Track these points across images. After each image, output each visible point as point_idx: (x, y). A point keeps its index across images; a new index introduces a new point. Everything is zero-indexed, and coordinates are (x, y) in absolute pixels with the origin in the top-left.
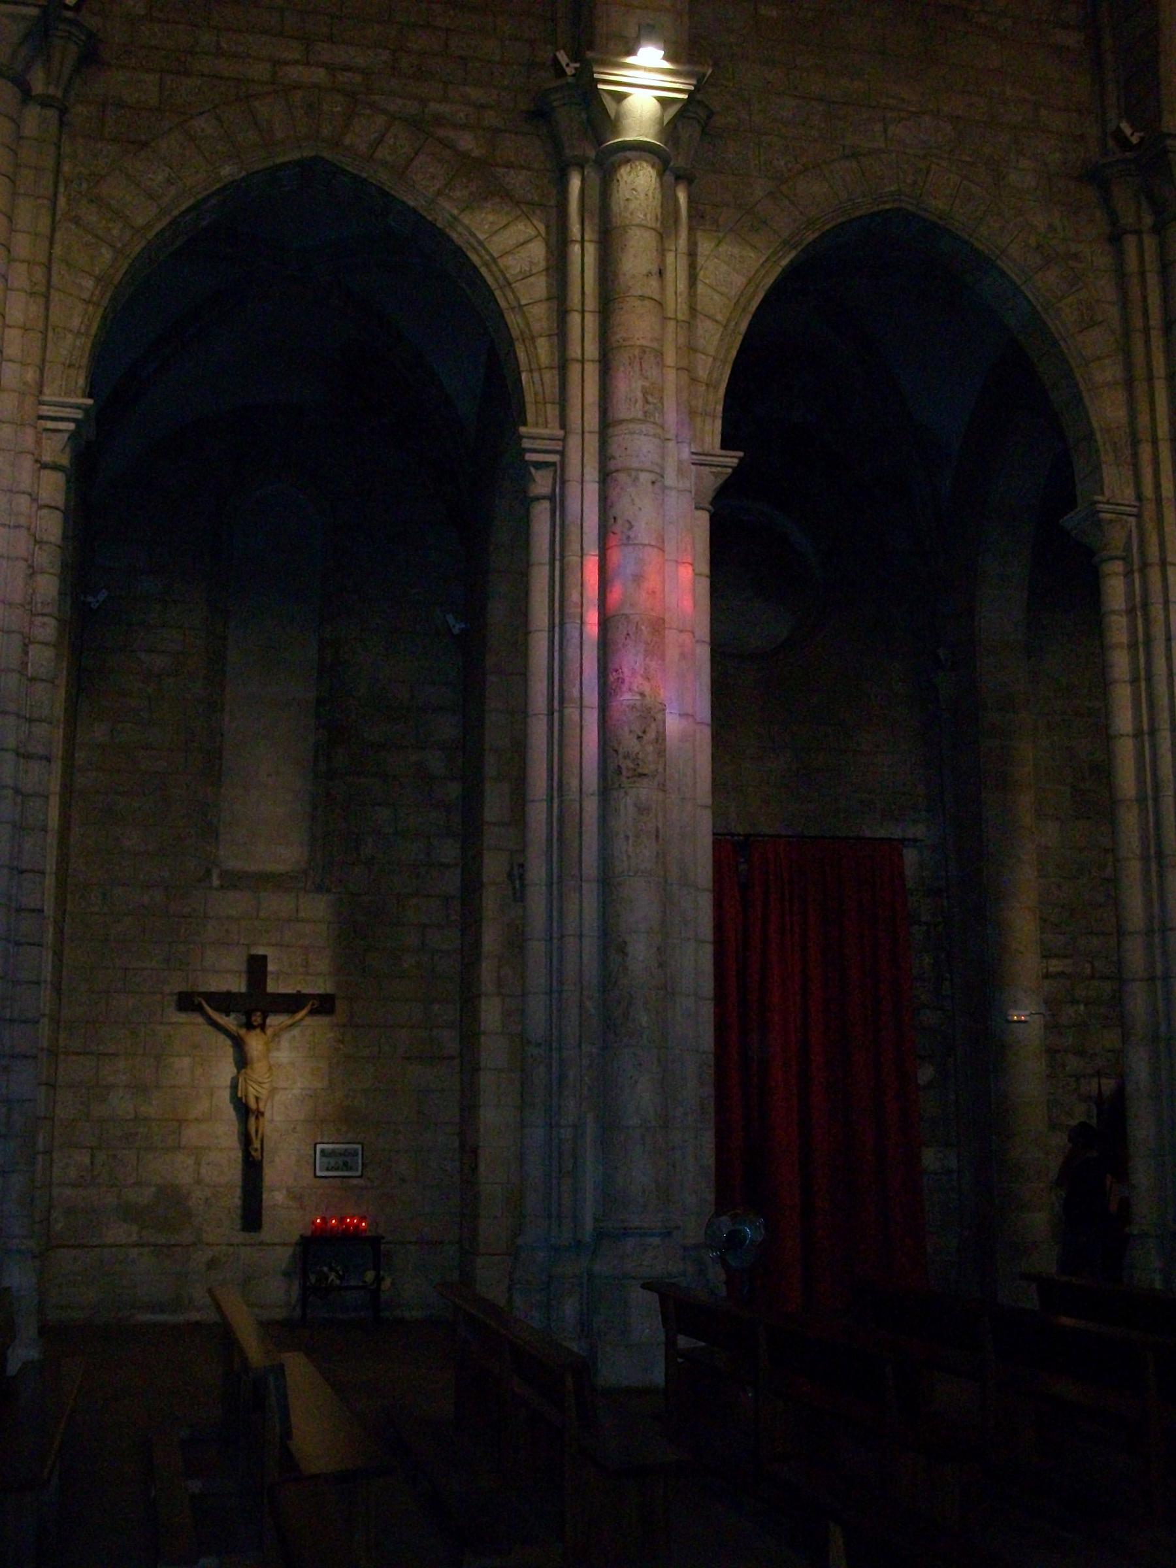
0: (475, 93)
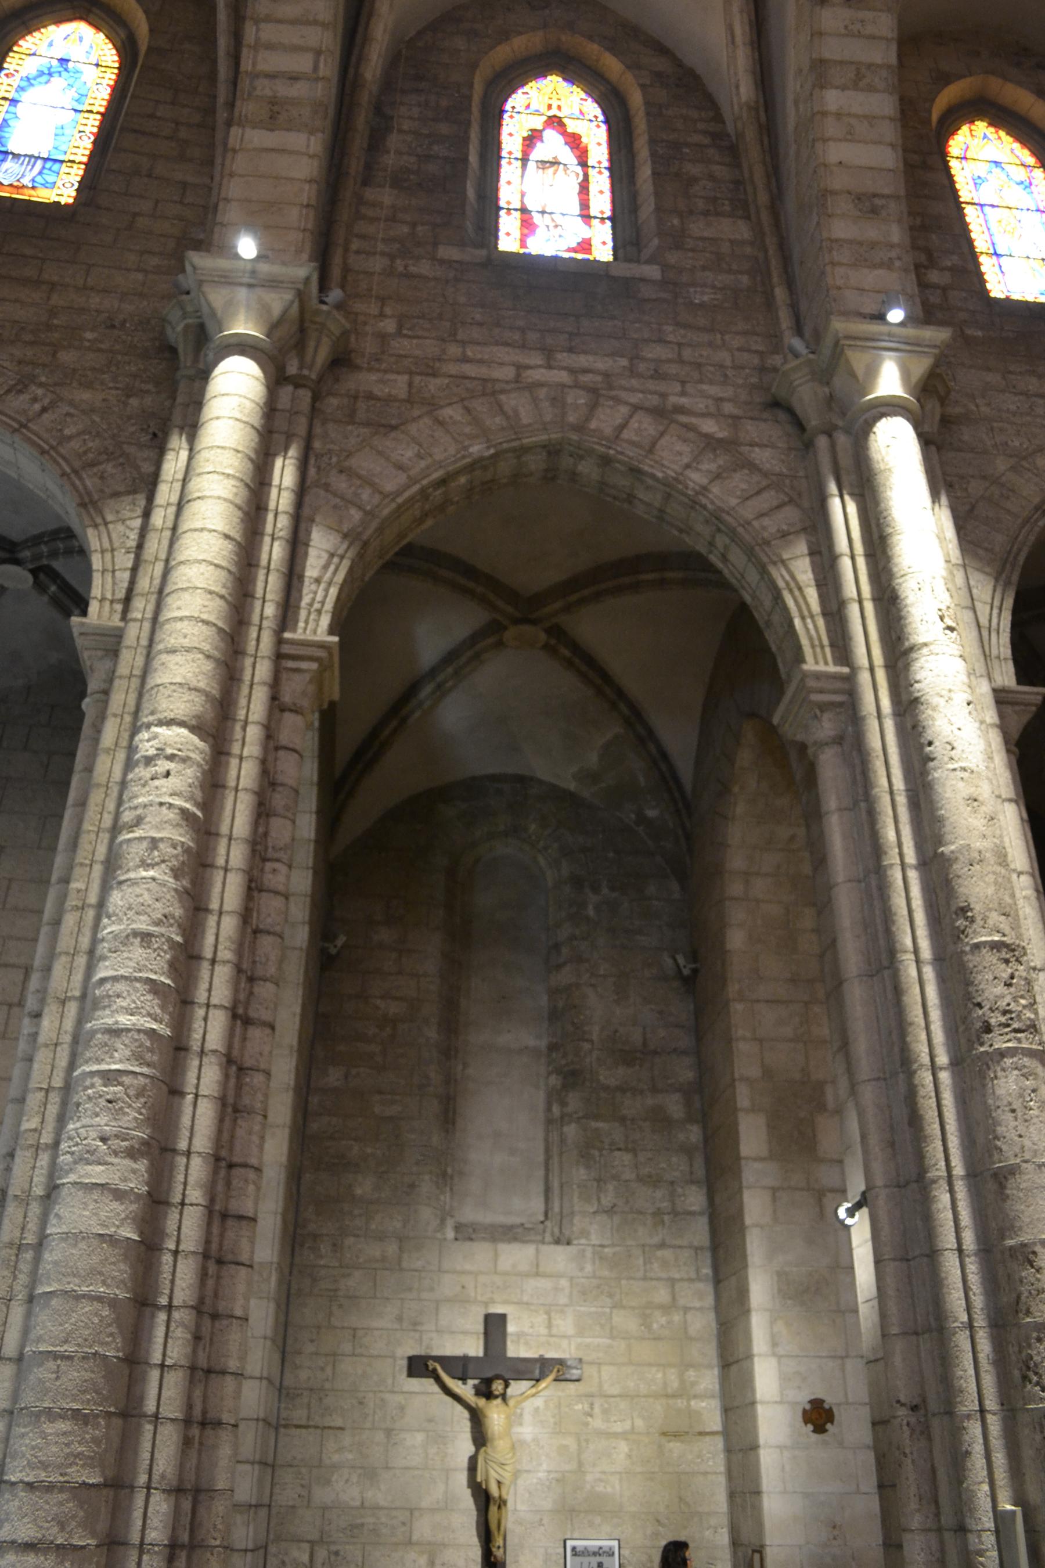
0: (713, 390)
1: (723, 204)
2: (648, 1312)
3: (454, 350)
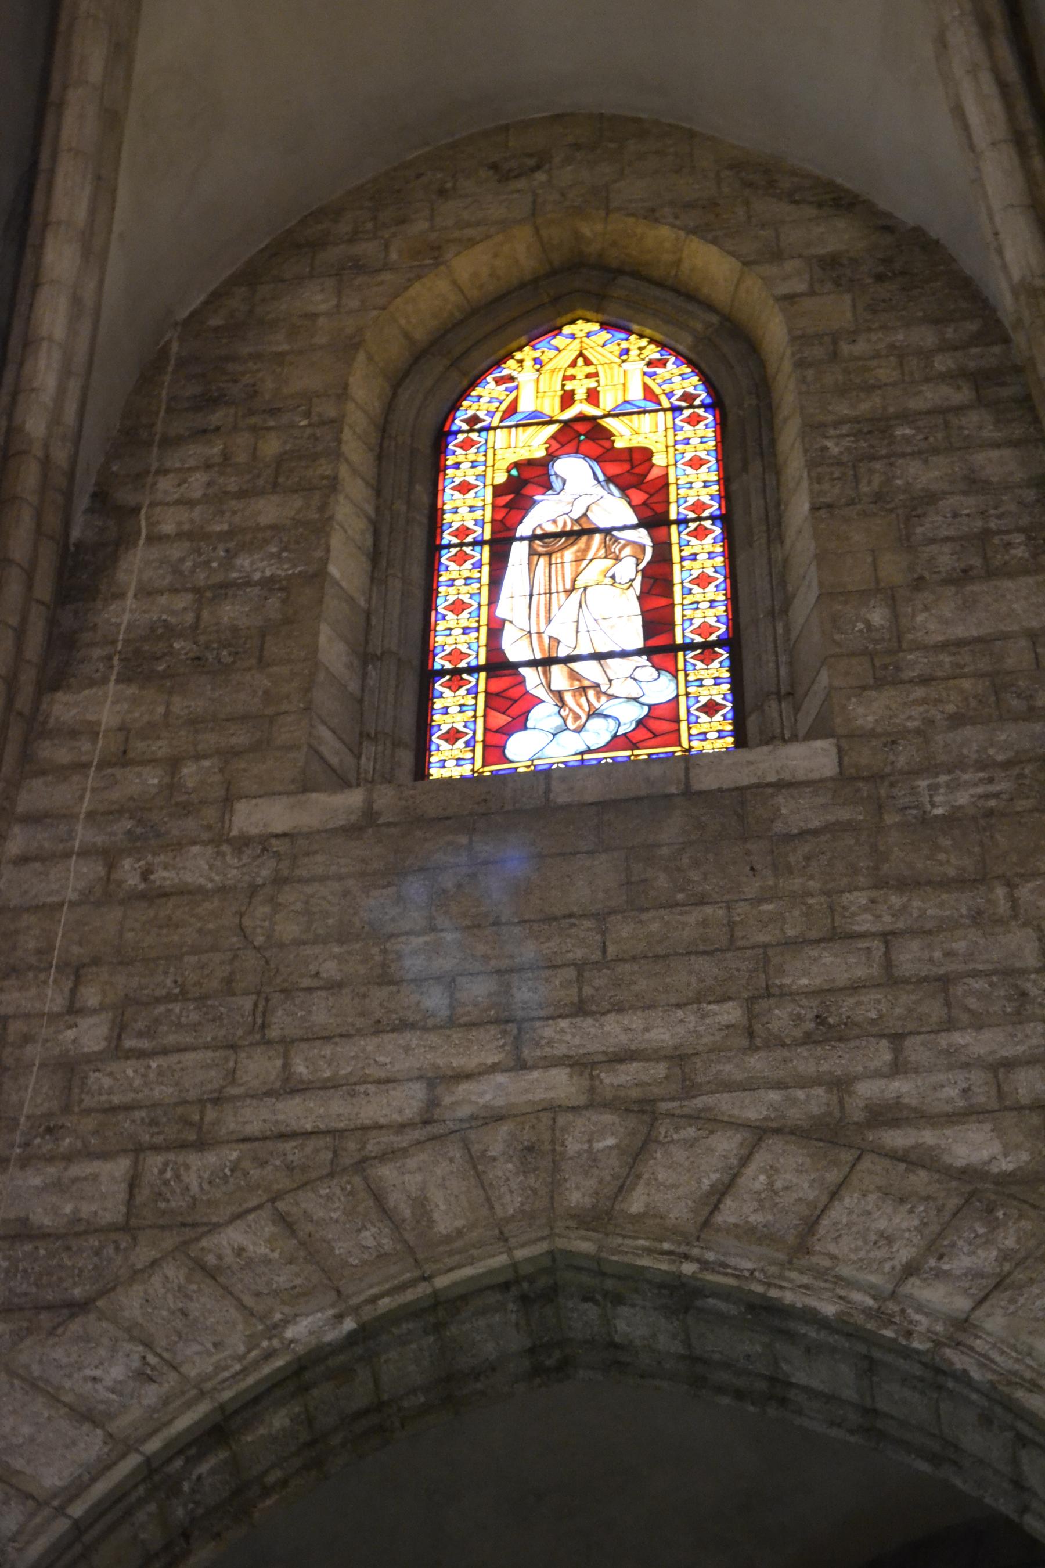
1: (1009, 545)
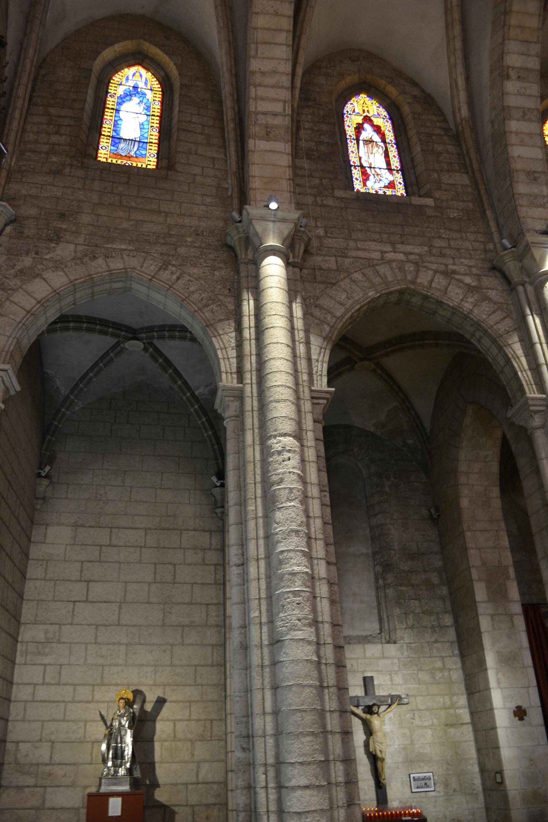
2: (434, 672)
3: (352, 244)
